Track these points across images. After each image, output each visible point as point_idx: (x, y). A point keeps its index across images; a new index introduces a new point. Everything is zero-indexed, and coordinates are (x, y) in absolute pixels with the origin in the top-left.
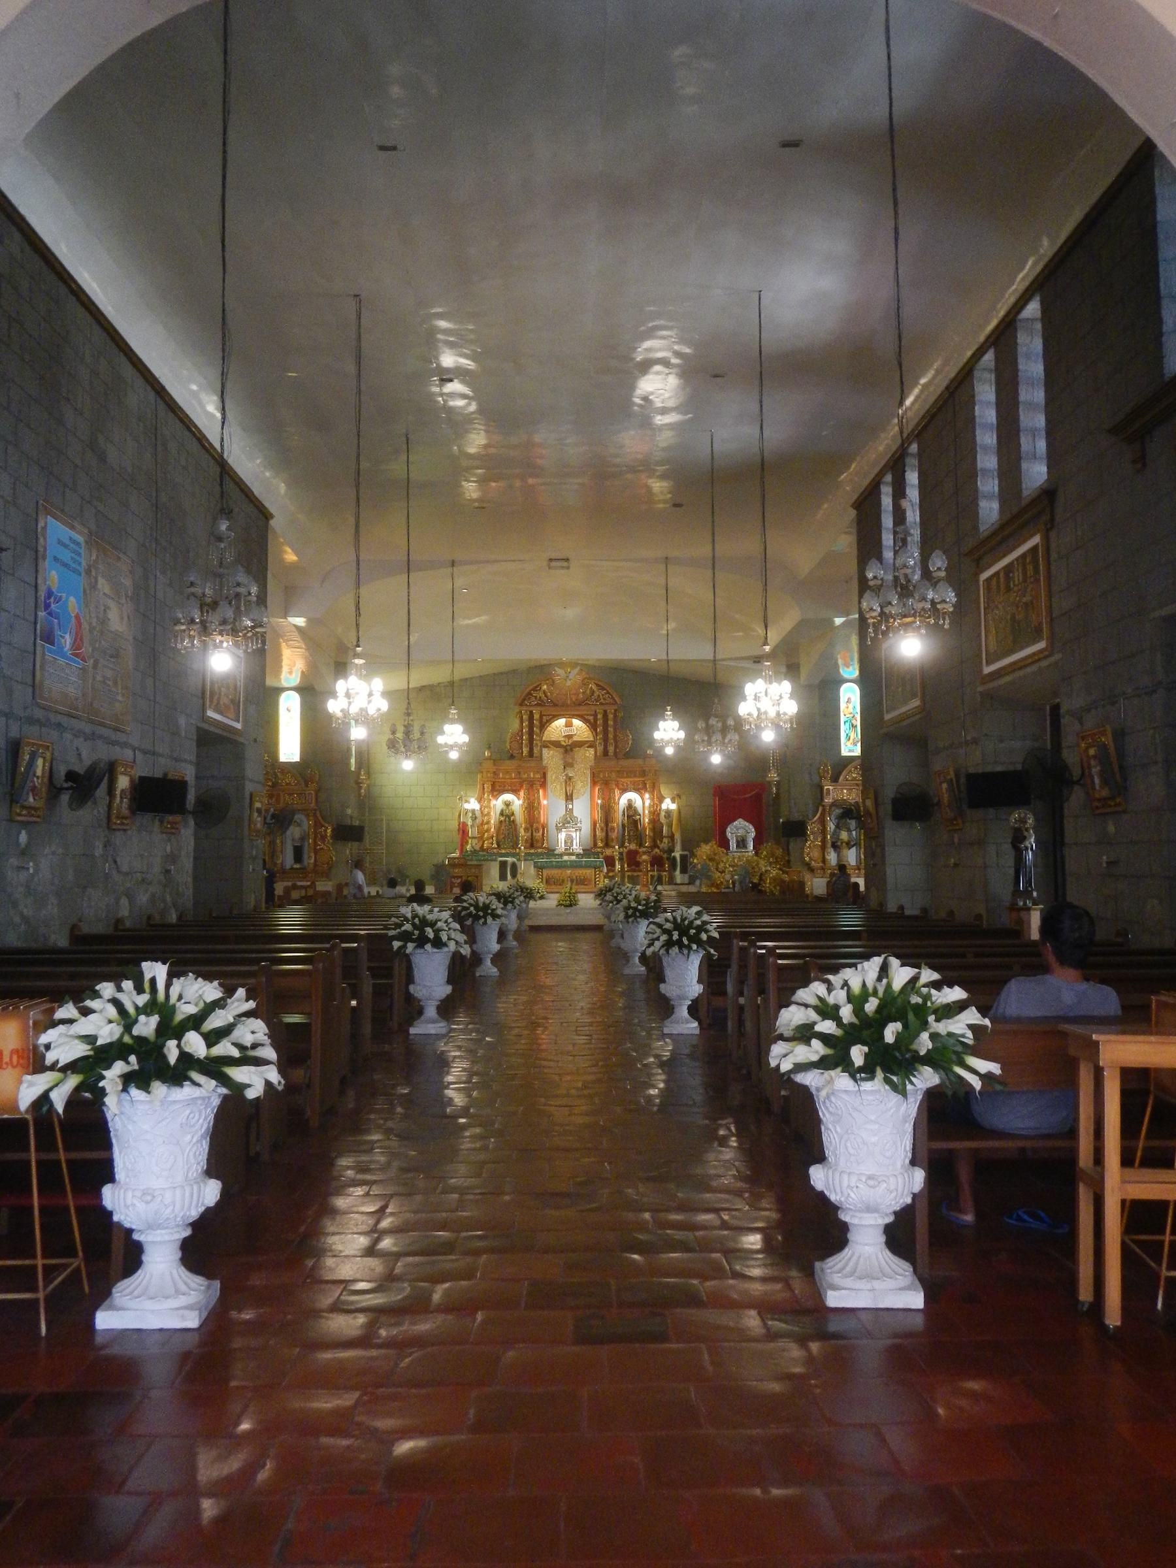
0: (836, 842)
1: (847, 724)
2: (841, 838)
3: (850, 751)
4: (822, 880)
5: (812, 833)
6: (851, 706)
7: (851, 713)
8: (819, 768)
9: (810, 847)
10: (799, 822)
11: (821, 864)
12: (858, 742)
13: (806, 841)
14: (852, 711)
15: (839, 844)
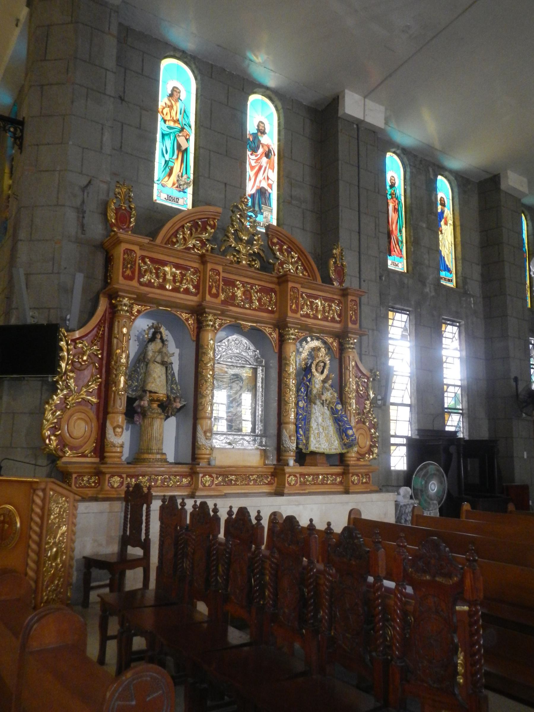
0: (141, 398)
1: (168, 143)
2: (151, 387)
3: (169, 198)
4: (94, 506)
5: (75, 368)
6: (178, 106)
7: (177, 121)
8: (105, 205)
9: (64, 406)
10: (36, 328)
11: (97, 460)
12: (188, 184)
13: (54, 390)
14: (179, 116)
15: (145, 403)
